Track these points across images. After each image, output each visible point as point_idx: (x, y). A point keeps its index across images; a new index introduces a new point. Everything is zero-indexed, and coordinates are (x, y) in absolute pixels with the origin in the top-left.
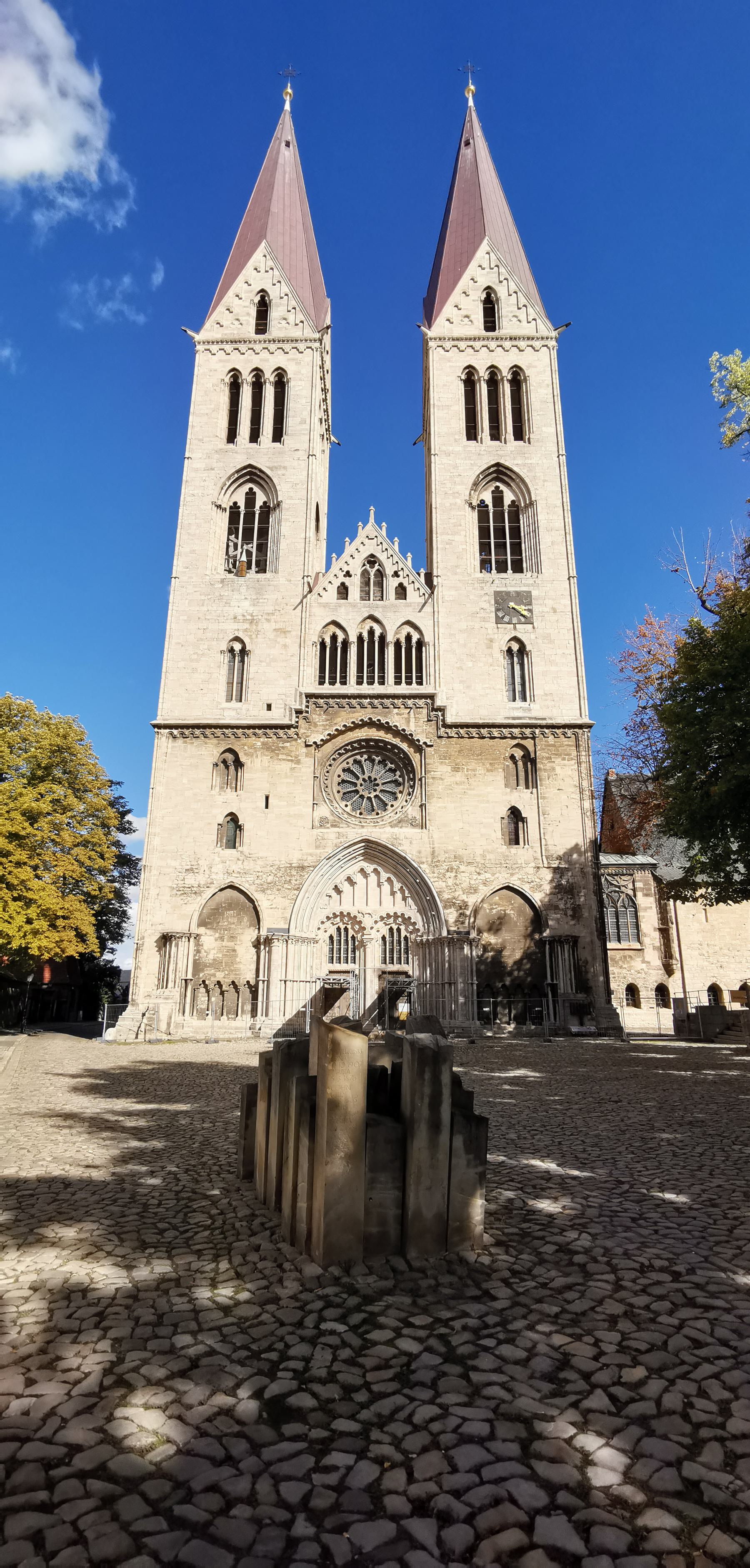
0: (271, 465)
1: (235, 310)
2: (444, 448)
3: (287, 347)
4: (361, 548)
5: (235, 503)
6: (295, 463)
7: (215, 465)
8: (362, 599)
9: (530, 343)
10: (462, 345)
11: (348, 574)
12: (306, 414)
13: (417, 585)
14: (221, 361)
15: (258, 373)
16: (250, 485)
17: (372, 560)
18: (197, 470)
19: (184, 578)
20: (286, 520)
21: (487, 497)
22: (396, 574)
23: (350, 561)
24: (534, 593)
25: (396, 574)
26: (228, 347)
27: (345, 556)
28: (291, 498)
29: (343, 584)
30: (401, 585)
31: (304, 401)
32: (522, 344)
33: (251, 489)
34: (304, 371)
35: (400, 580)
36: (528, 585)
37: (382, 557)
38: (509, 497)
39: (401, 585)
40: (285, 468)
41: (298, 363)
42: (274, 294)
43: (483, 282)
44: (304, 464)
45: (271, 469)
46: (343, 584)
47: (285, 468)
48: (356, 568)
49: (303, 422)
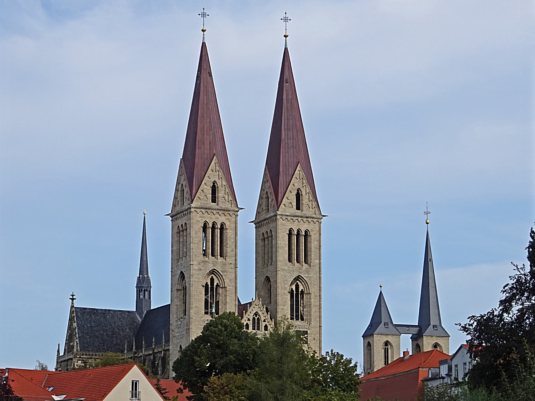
0: (222, 270)
1: (205, 191)
2: (281, 267)
3: (226, 213)
4: (254, 309)
5: (207, 283)
6: (231, 270)
7: (202, 268)
8: (253, 329)
9: (313, 220)
10: (289, 218)
11: (249, 320)
12: (234, 246)
13: (272, 326)
14: (201, 217)
15: (214, 224)
16: (213, 275)
17: (256, 314)
18: (195, 270)
19: (194, 318)
20: (229, 296)
21: (294, 287)
22: (264, 321)
23: (250, 314)
24: (308, 332)
25: (264, 321)
26: (203, 210)
27: (248, 313)
28: (229, 286)
29: (247, 323)
30: (266, 325)
31: (232, 240)
32: (310, 220)
33: (212, 277)
34: (232, 225)
35: (266, 323)
36: (306, 328)
37: (260, 313)
38: (301, 288)
39: (266, 325)
40: (227, 272)
41: (229, 221)
42: (219, 183)
43: (297, 186)
44: (234, 271)
45: (222, 272)
46: (247, 323)
47: (227, 272)
48: (251, 319)
49: (232, 251)
